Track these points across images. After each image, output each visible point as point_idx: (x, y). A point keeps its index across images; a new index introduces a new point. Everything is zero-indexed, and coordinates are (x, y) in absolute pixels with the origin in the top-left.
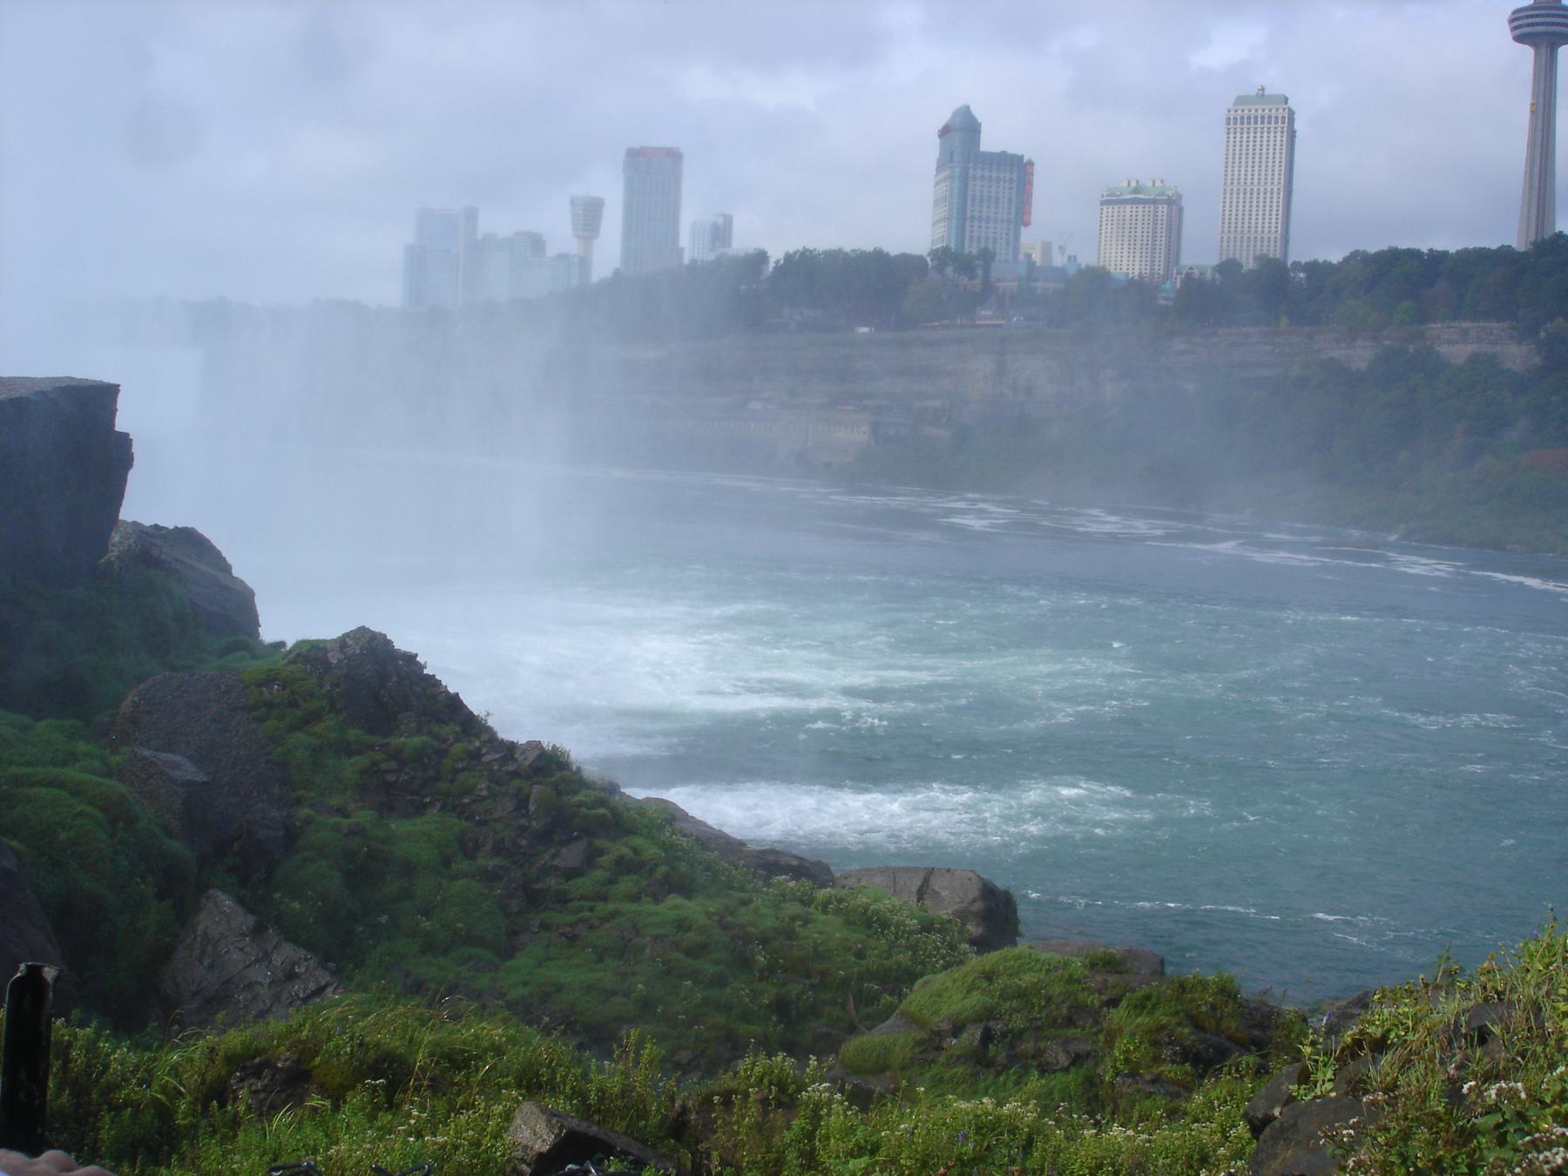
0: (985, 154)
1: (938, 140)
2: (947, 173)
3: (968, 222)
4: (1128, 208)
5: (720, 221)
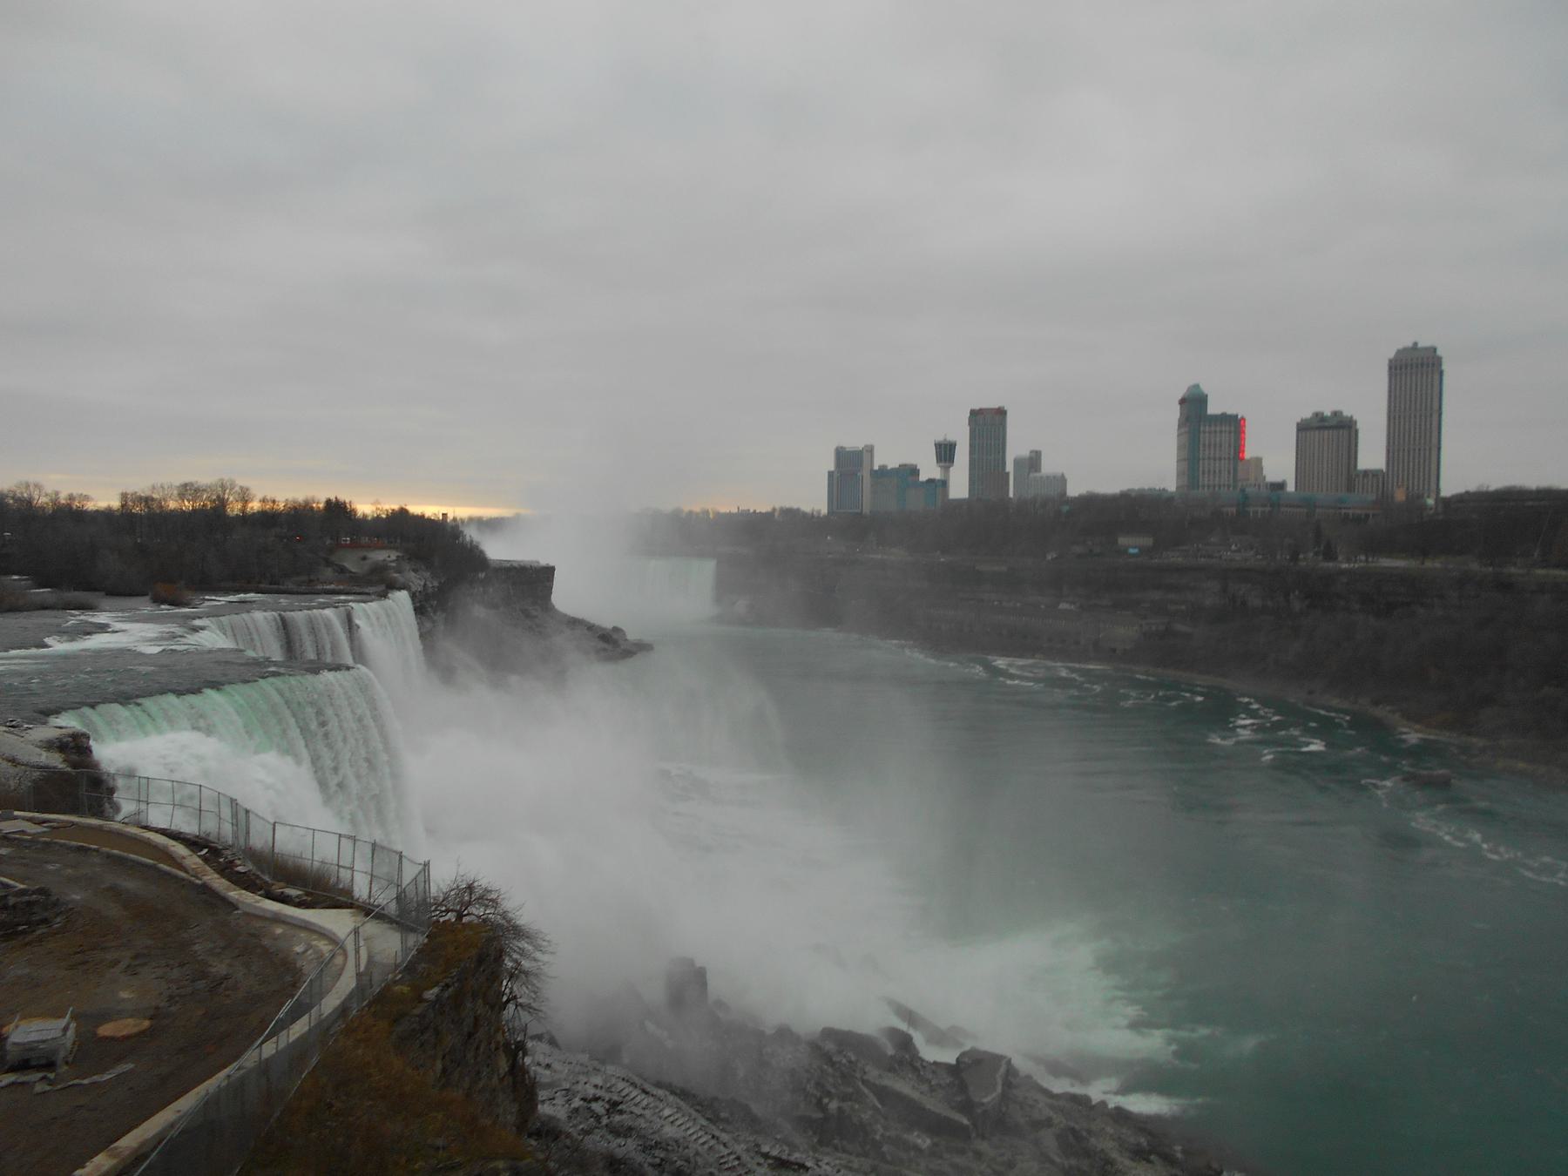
0: (1210, 416)
1: (1178, 407)
2: (1187, 429)
3: (1201, 462)
4: (1317, 432)
5: (1033, 455)
